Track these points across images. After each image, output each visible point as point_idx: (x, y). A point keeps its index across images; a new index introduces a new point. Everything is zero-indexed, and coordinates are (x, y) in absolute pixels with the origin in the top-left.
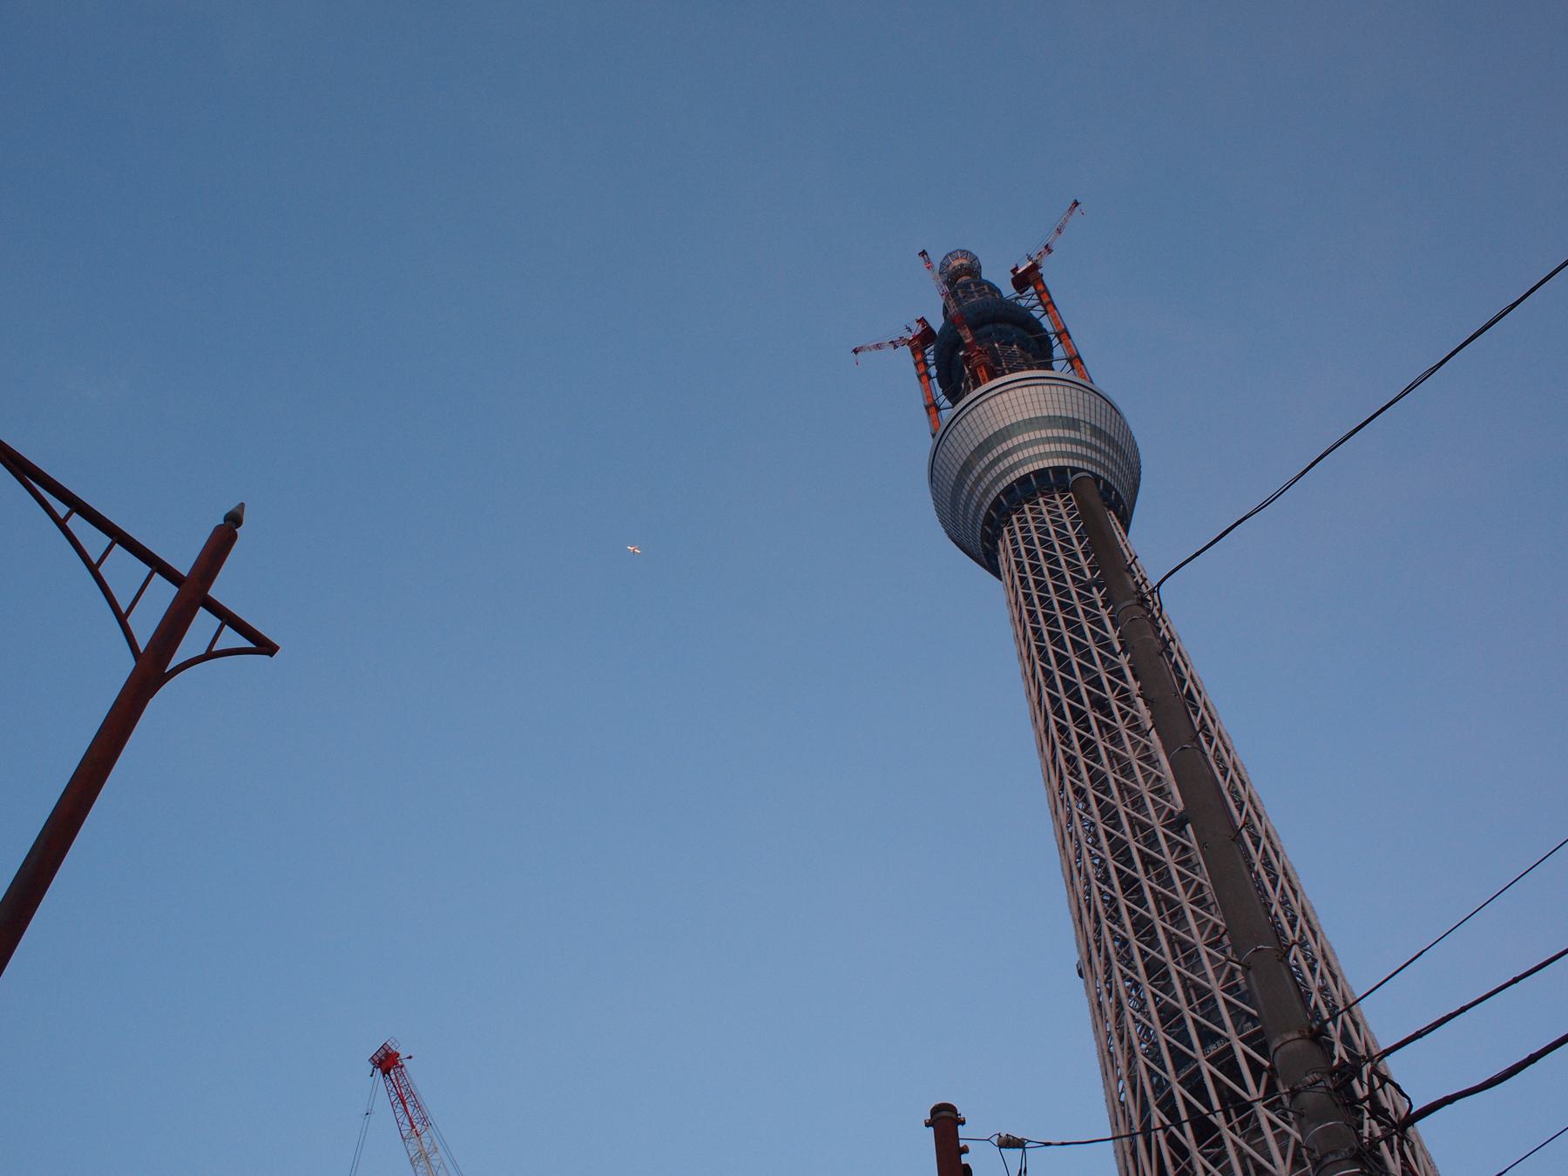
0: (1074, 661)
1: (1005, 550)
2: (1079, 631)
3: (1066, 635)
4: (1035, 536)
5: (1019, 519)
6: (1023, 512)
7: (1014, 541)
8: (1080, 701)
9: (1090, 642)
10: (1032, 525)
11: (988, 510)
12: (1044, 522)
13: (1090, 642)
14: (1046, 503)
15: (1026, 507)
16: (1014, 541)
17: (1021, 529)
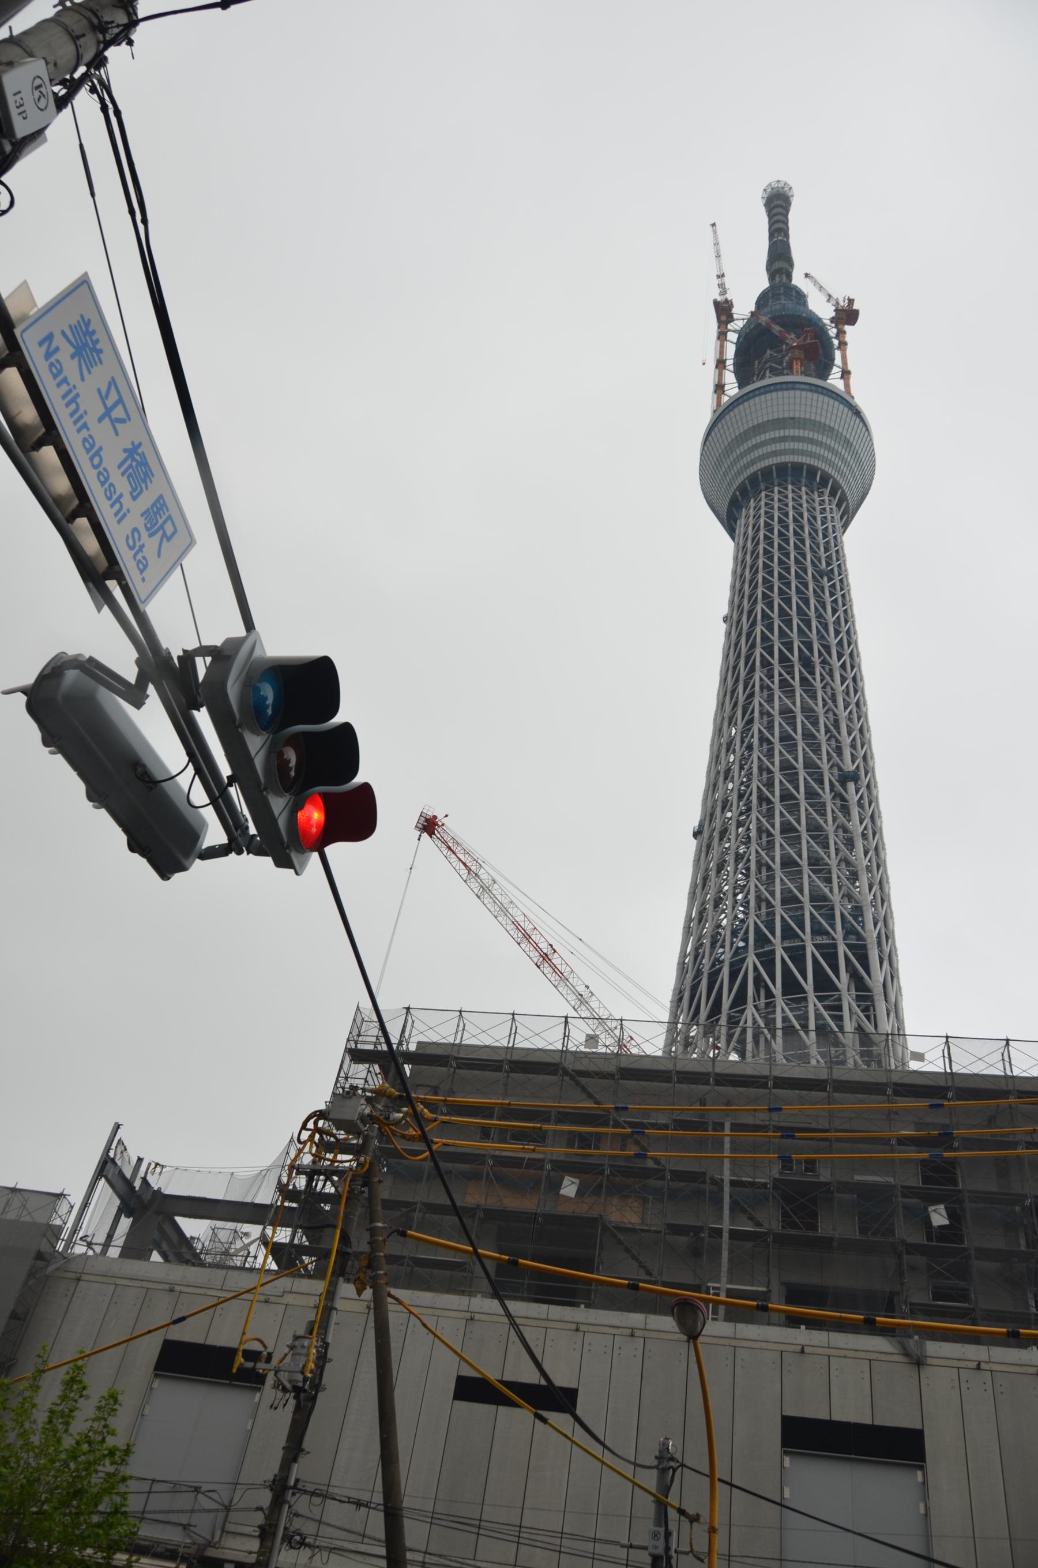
0: (777, 623)
1: (747, 517)
2: (788, 601)
3: (777, 601)
4: (776, 515)
5: (767, 496)
6: (773, 492)
7: (757, 517)
8: (772, 655)
9: (794, 612)
10: (776, 505)
11: (745, 480)
12: (787, 505)
13: (794, 612)
14: (793, 491)
15: (776, 489)
16: (757, 517)
17: (766, 504)
